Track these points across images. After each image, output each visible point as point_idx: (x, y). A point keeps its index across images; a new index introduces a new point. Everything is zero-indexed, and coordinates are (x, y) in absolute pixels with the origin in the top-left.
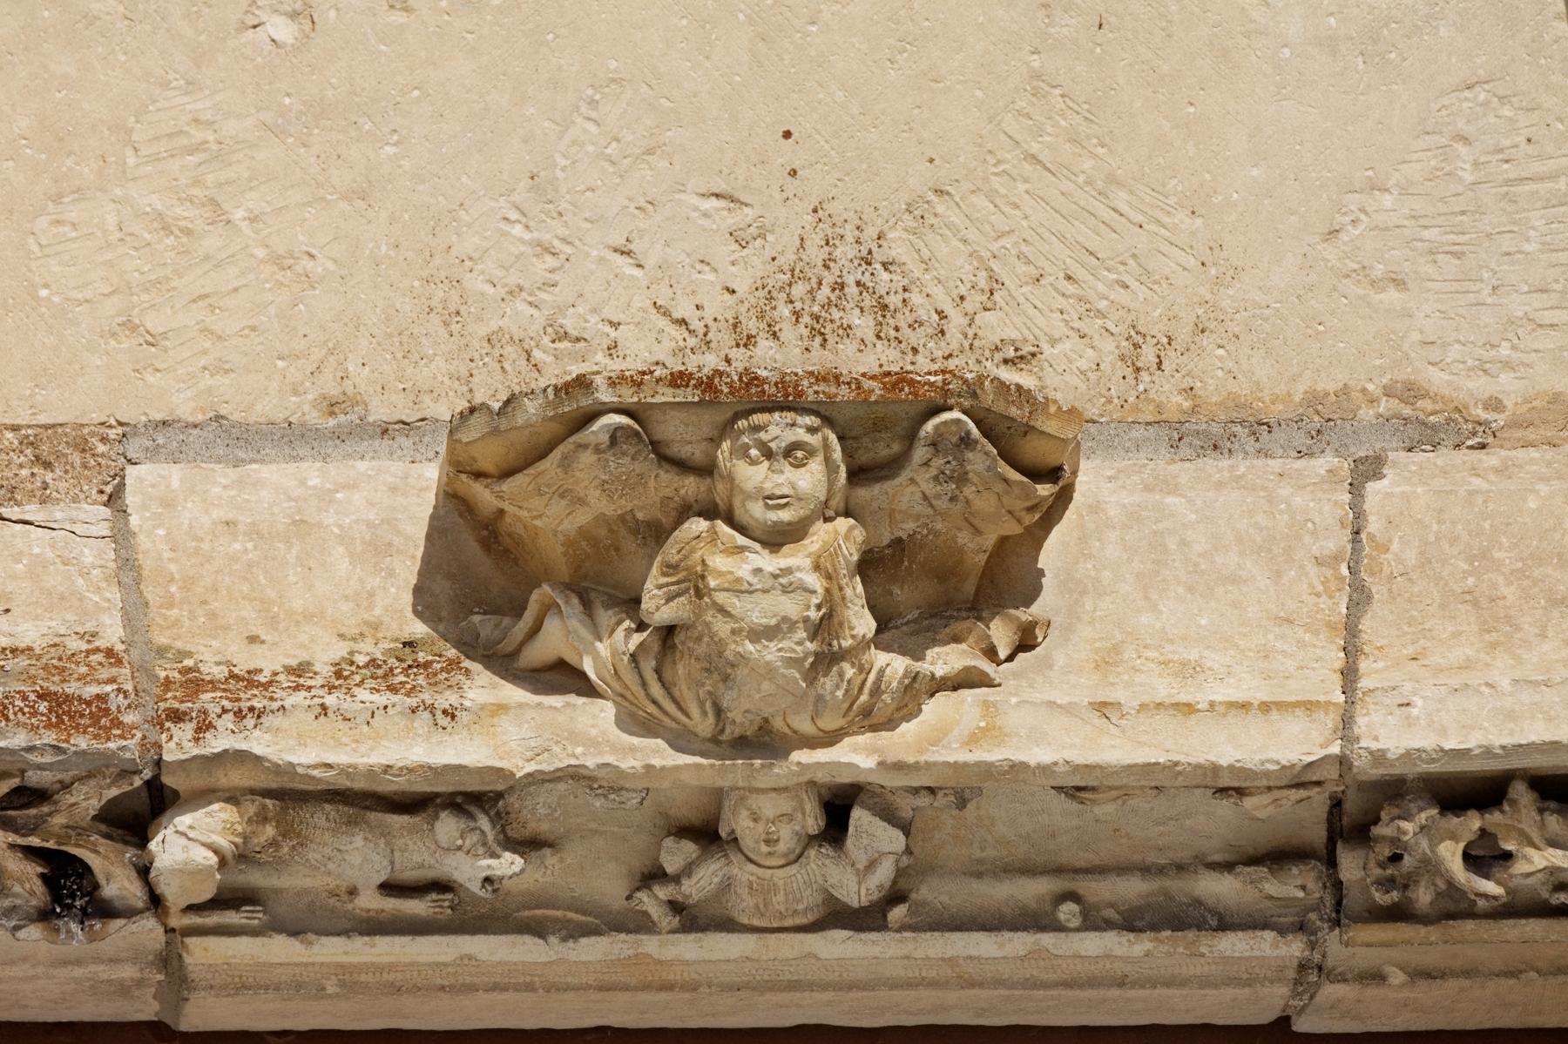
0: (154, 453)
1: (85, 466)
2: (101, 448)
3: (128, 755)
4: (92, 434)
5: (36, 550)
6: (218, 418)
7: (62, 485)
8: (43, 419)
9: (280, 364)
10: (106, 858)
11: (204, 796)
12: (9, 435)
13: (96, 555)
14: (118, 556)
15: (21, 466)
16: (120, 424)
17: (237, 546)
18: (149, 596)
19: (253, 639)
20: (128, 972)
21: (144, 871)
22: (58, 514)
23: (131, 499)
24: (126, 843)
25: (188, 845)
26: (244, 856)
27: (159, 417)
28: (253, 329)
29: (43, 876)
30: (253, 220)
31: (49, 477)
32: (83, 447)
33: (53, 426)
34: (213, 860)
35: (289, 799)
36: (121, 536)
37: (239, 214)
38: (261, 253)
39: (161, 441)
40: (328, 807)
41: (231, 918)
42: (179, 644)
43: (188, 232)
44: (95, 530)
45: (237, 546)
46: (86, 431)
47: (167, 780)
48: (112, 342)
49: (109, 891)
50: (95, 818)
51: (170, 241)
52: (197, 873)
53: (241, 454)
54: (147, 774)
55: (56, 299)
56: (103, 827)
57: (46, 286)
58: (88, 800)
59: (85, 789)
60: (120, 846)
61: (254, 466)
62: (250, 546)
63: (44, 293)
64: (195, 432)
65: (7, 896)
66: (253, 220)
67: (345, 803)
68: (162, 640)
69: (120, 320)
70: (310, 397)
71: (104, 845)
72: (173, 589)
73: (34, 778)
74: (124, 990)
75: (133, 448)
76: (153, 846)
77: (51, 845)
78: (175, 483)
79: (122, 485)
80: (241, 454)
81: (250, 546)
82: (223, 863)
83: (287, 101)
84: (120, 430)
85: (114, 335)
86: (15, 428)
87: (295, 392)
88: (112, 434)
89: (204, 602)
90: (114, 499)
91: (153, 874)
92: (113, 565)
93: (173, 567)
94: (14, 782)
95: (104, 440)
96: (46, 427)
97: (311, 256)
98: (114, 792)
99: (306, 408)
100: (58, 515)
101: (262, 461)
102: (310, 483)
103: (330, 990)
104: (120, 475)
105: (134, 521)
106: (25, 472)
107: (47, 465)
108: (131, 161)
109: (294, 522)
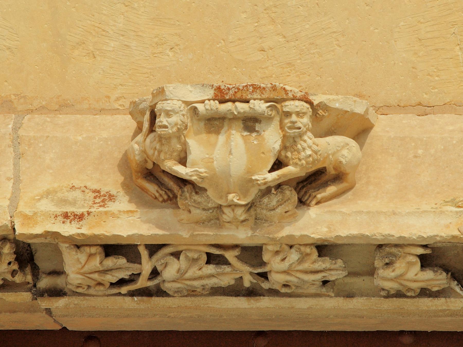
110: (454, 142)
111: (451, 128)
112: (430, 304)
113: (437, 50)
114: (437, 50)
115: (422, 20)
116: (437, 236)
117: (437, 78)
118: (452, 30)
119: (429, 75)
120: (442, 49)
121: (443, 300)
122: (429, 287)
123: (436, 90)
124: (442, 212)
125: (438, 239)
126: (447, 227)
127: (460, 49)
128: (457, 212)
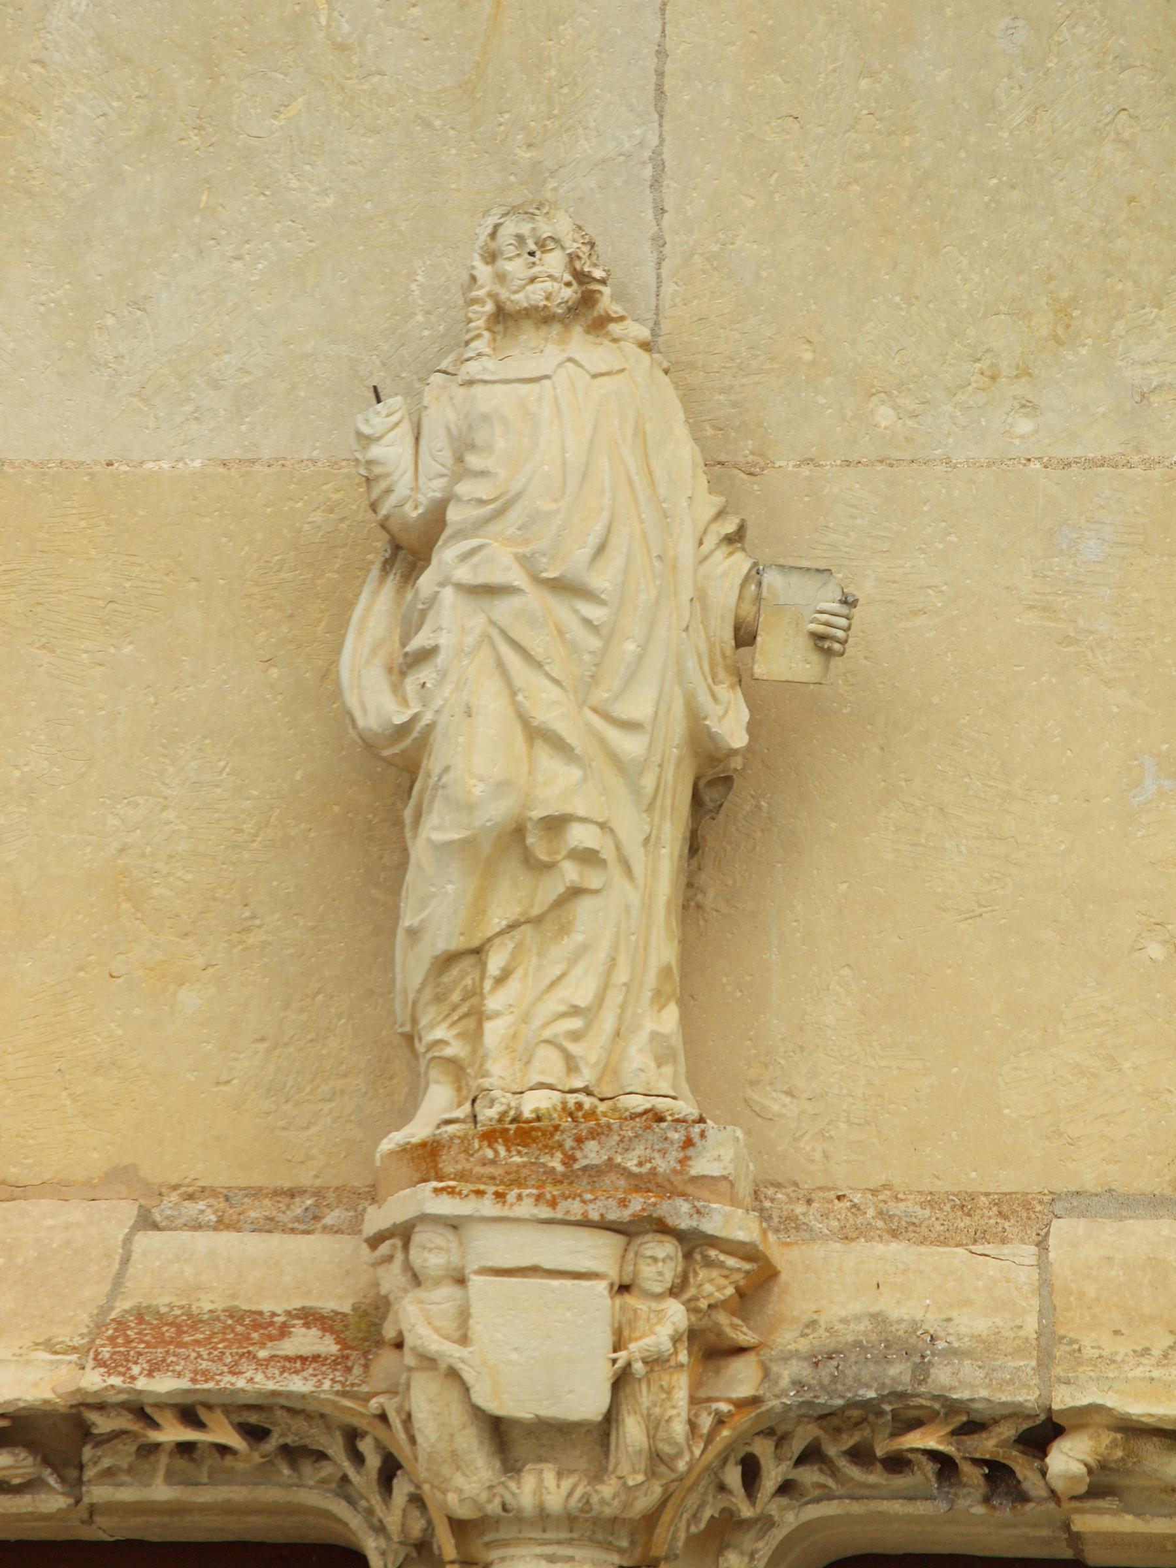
0: (1071, 1212)
1: (1029, 1218)
2: (1039, 1208)
3: (1029, 1405)
4: (1033, 1199)
5: (991, 1273)
6: (1110, 1191)
7: (1016, 1230)
8: (1004, 1189)
9: (1150, 1158)
10: (1022, 1466)
11: (1080, 1427)
12: (983, 1199)
13: (1026, 1276)
14: (1040, 1278)
15: (990, 1218)
16: (1051, 1193)
17: (1113, 1273)
18: (1057, 1304)
19: (1117, 1333)
20: (1045, 1532)
21: (1043, 1473)
22: (1006, 1250)
23: (1052, 1241)
24: (1035, 1456)
25: (1067, 1460)
26: (1103, 1466)
27: (1074, 1189)
28: (1133, 1136)
29: (986, 1476)
30: (1136, 1068)
31: (1007, 1224)
32: (1028, 1207)
33: (1010, 1194)
34: (1084, 1470)
35: (1134, 1431)
36: (1043, 1264)
37: (1127, 1065)
38: (1139, 1089)
39: (1075, 1204)
40: (1155, 1439)
41: (1101, 1503)
42: (1071, 1335)
43: (1095, 1075)
44: (1028, 1261)
45: (1113, 1273)
46: (1030, 1196)
47: (1055, 1419)
48: (1047, 1143)
49: (1026, 1486)
50: (1015, 1441)
51: (1085, 1081)
52: (1074, 1479)
53: (1124, 1213)
54: (1043, 1417)
55: (1014, 1115)
56: (1021, 1447)
57: (1008, 1107)
58: (1008, 1431)
59: (1007, 1424)
60: (1030, 1458)
61: (1131, 1221)
62: (1121, 1273)
63: (1007, 1111)
64: (1097, 1199)
65: (965, 1486)
66: (1136, 1068)
67: (1166, 1437)
68: (1062, 1332)
69: (1053, 1129)
70: (1167, 1178)
71: (1021, 1459)
72: (1072, 1299)
73: (977, 1417)
74: (1044, 1541)
75: (1058, 1208)
76: (1048, 1460)
77: (987, 1457)
78: (1080, 1232)
79: (1048, 1234)
80: (1124, 1213)
81: (1121, 1273)
82: (1090, 1471)
83: (1158, 996)
84: (1050, 1197)
85: (1048, 1138)
86: (987, 1195)
87: (1158, 1176)
88: (1046, 1199)
89: (1090, 1308)
90: (1042, 1244)
91: (1048, 1477)
92: (1037, 1283)
93: (1073, 1285)
94: (965, 1419)
95: (1041, 1202)
96: (1006, 1194)
97: (1170, 1091)
98: (1025, 1426)
99: (1164, 1185)
100: (1006, 1251)
101: (1137, 1218)
102: (1163, 1233)
103: (1169, 1548)
104: (1048, 1225)
105: (1052, 1255)
106: (992, 1221)
107: (1006, 1218)
108: (1062, 1031)
109: (1149, 1259)
110: (55, 1246)
111: (51, 1222)
112: (8, 1504)
113: (32, 1096)
114: (32, 1096)
115: (10, 1049)
116: (19, 1400)
117: (31, 1142)
118: (57, 1066)
119: (18, 1136)
120: (40, 1095)
121: (28, 1498)
122: (7, 1479)
123: (30, 1161)
124: (28, 1362)
125: (21, 1404)
126: (35, 1385)
127: (70, 1095)
128: (52, 1362)
